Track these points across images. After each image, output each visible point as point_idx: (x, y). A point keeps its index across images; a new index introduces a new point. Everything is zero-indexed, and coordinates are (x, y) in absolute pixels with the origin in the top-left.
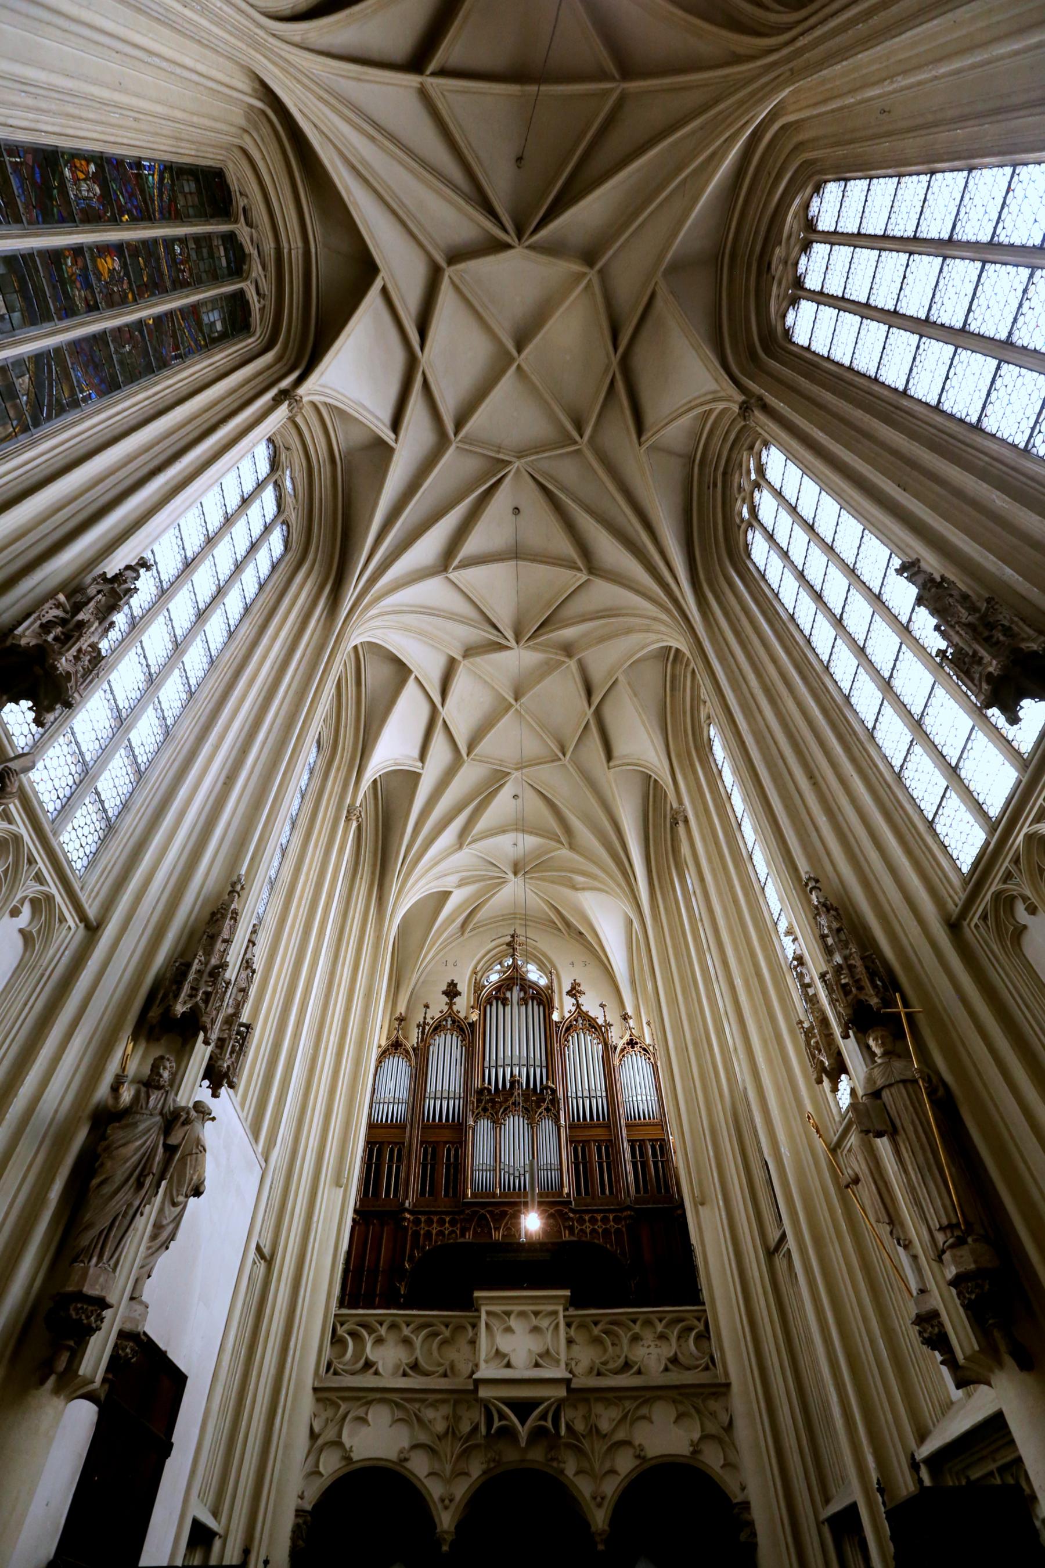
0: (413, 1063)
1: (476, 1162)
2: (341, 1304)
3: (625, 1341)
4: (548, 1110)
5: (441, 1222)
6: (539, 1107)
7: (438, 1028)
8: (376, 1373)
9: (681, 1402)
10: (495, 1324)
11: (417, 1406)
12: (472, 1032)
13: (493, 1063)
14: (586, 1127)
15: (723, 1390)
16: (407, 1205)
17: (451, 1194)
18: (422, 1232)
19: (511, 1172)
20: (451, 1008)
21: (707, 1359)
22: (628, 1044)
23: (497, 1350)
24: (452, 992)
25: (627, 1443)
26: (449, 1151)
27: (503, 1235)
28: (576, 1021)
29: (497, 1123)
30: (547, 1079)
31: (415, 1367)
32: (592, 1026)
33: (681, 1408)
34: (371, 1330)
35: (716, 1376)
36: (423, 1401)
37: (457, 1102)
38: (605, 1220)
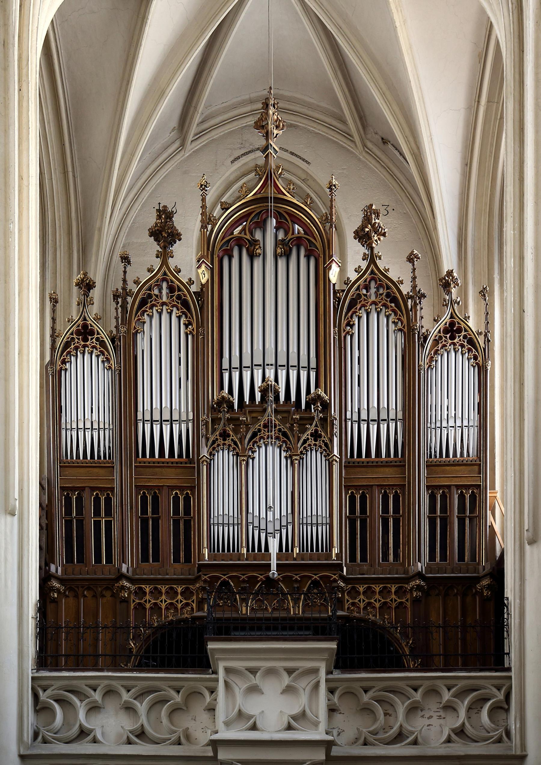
1: (215, 513)
4: (316, 436)
12: (201, 308)
13: (236, 363)
14: (370, 465)
17: (182, 559)
19: (263, 526)
20: (165, 263)
22: (446, 331)
23: (240, 710)
24: (165, 233)
26: (176, 499)
28: (367, 288)
30: (317, 386)
31: (141, 734)
35: (510, 748)
38: (385, 592)
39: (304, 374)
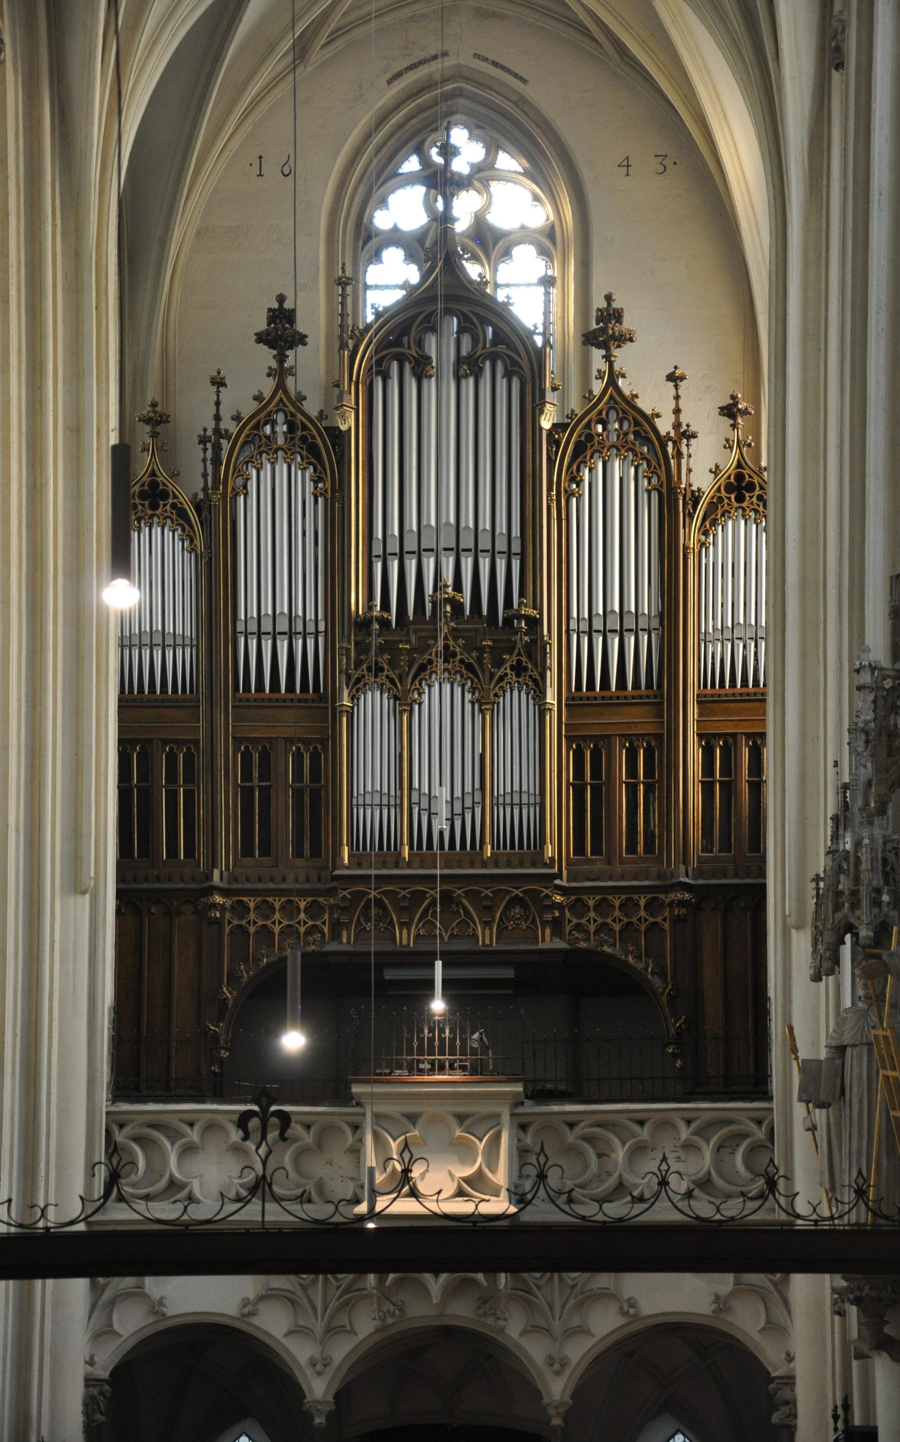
5: (289, 909)
6: (498, 663)
20: (281, 385)
26: (298, 757)
27: (418, 936)
29: (403, 703)
37: (310, 643)
39: (501, 565)
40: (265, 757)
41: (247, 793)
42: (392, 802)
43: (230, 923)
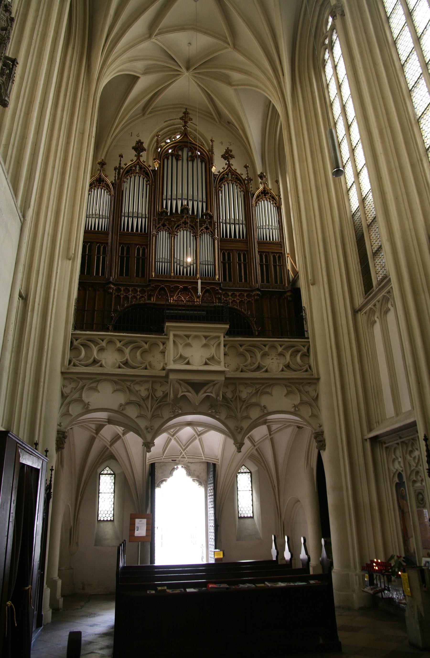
0: (113, 193)
1: (158, 257)
2: (75, 328)
3: (259, 355)
4: (207, 228)
6: (201, 226)
7: (129, 171)
8: (101, 366)
9: (289, 386)
10: (178, 341)
11: (129, 384)
13: (169, 197)
15: (315, 381)
16: (111, 279)
18: (122, 296)
19: (182, 264)
21: (307, 366)
25: (257, 405)
28: (228, 175)
32: (237, 179)
33: (289, 389)
34: (96, 343)
36: (132, 381)
37: (143, 220)
38: (241, 295)
40: (128, 249)
41: (122, 258)
42: (168, 261)
43: (115, 294)
